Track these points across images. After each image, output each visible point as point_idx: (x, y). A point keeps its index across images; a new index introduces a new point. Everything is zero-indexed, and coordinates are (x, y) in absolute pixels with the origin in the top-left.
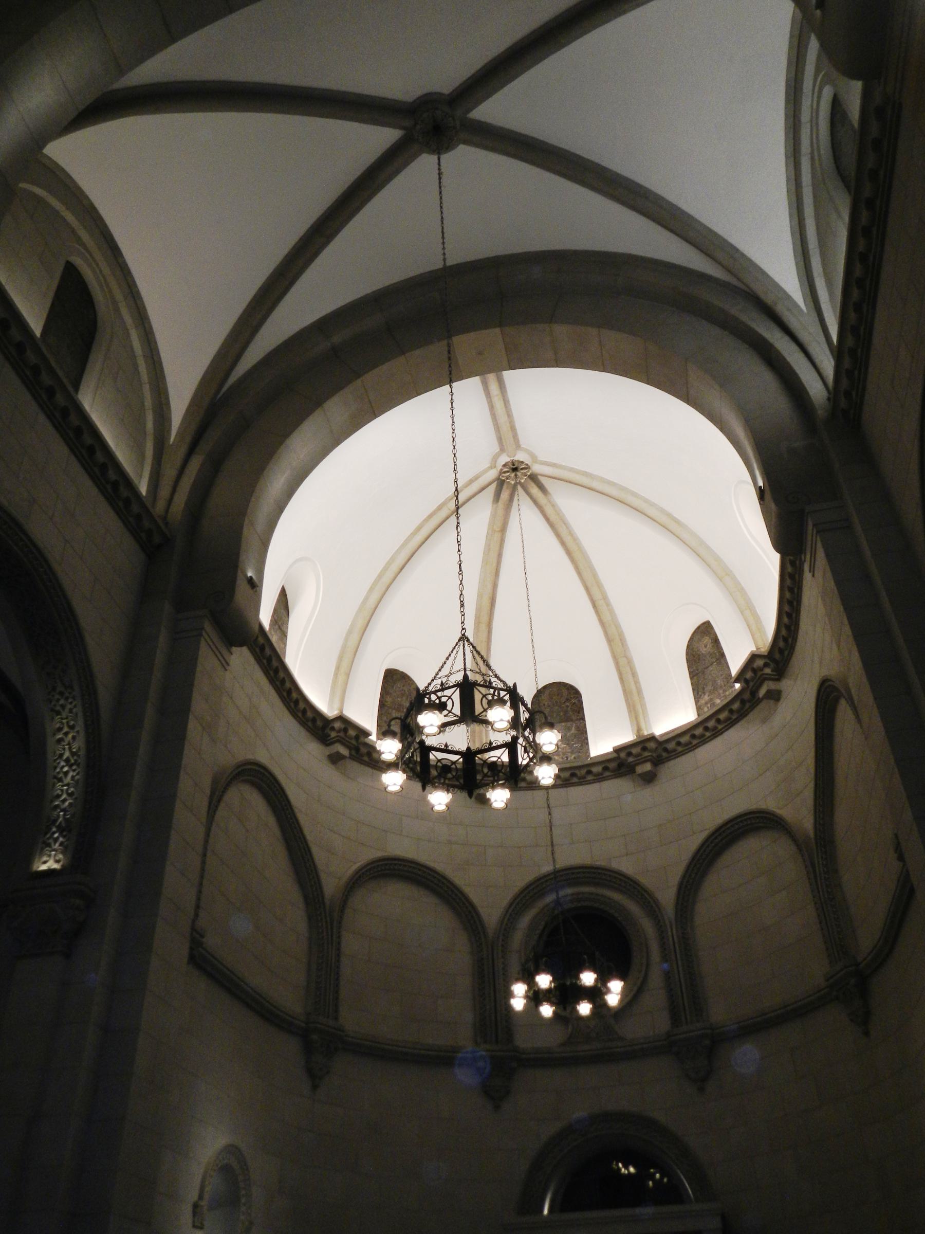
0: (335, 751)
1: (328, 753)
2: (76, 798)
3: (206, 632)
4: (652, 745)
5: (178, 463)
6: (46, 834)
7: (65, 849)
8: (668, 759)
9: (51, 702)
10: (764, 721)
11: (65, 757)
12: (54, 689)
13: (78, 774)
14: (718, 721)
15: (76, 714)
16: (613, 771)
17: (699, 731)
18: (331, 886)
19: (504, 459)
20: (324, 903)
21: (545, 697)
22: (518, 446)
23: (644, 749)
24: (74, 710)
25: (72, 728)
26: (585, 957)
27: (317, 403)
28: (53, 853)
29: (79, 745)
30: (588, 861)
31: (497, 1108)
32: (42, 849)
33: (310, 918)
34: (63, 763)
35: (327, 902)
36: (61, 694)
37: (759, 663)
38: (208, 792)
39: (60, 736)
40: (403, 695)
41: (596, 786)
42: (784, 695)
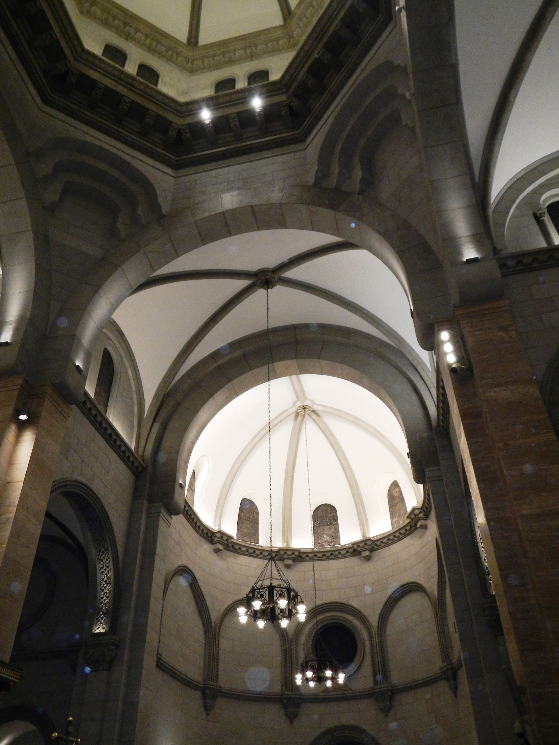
0: (217, 547)
1: (213, 548)
2: (110, 599)
3: (162, 513)
4: (369, 543)
5: (149, 428)
6: (98, 615)
8: (377, 549)
9: (99, 555)
10: (420, 537)
12: (100, 550)
13: (110, 588)
14: (400, 533)
16: (351, 553)
17: (391, 537)
18: (214, 616)
19: (299, 404)
20: (212, 625)
21: (320, 511)
22: (305, 397)
24: (109, 560)
26: (328, 663)
27: (211, 395)
28: (101, 624)
29: (111, 574)
30: (338, 600)
31: (292, 722)
32: (96, 623)
33: (205, 633)
34: (104, 583)
35: (213, 624)
36: (103, 552)
37: (417, 512)
38: (163, 588)
39: (103, 570)
40: (250, 512)
41: (343, 560)
42: (428, 527)
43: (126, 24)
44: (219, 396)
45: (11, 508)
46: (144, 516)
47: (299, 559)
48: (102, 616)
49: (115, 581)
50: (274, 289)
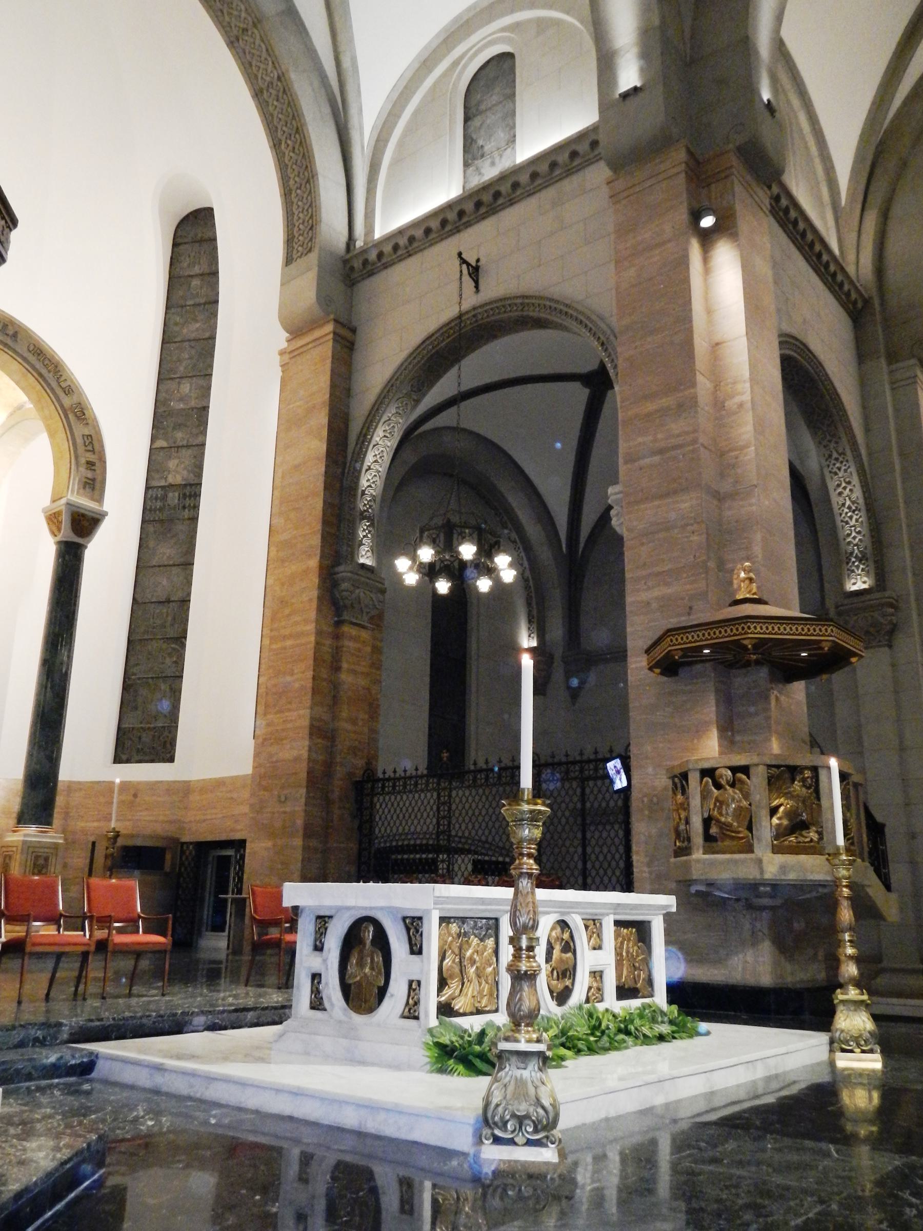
6: (848, 563)
7: (868, 574)
9: (828, 466)
11: (847, 505)
12: (830, 456)
15: (851, 473)
29: (858, 494)
32: (849, 575)
34: (846, 510)
36: (837, 459)
39: (840, 490)
45: (739, 387)
46: (887, 387)
48: (856, 564)
49: (866, 504)
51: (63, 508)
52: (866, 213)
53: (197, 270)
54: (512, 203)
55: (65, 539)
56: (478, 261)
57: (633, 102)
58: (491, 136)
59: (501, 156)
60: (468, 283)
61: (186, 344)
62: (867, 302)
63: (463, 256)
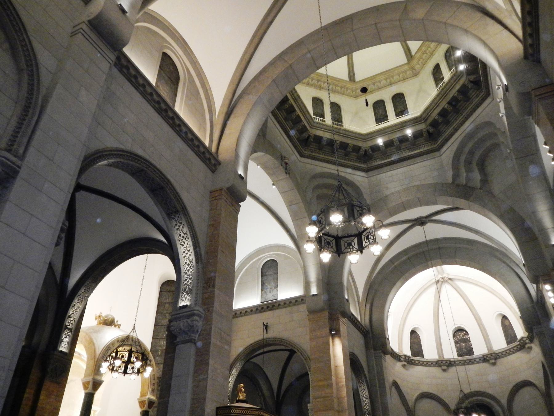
4: (494, 355)
5: (364, 308)
8: (499, 358)
12: (359, 381)
18: (411, 404)
19: (440, 276)
23: (492, 356)
25: (365, 390)
29: (367, 393)
36: (361, 382)
37: (525, 339)
39: (362, 391)
41: (478, 365)
43: (318, 81)
44: (398, 284)
47: (450, 365)
49: (369, 396)
50: (426, 225)
51: (147, 400)
52: (367, 304)
53: (167, 301)
54: (278, 309)
55: (146, 410)
56: (267, 323)
57: (315, 298)
58: (270, 283)
59: (273, 291)
60: (265, 331)
61: (163, 327)
62: (367, 332)
63: (264, 324)
